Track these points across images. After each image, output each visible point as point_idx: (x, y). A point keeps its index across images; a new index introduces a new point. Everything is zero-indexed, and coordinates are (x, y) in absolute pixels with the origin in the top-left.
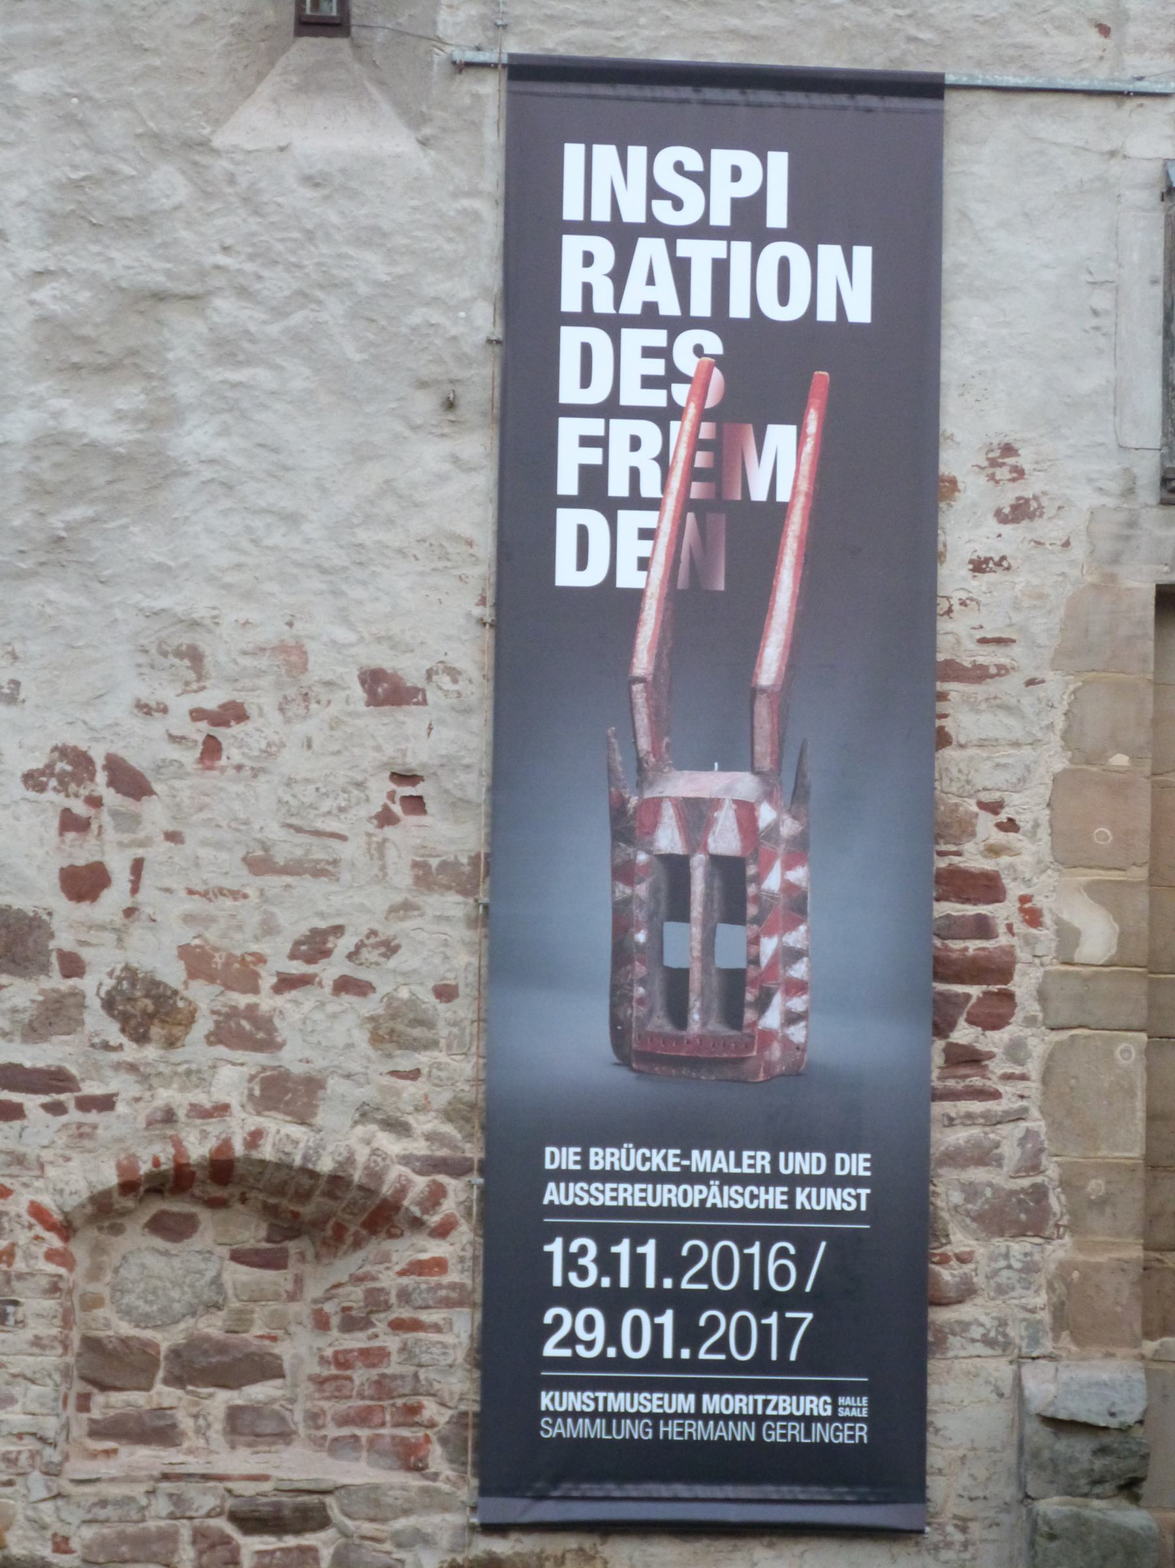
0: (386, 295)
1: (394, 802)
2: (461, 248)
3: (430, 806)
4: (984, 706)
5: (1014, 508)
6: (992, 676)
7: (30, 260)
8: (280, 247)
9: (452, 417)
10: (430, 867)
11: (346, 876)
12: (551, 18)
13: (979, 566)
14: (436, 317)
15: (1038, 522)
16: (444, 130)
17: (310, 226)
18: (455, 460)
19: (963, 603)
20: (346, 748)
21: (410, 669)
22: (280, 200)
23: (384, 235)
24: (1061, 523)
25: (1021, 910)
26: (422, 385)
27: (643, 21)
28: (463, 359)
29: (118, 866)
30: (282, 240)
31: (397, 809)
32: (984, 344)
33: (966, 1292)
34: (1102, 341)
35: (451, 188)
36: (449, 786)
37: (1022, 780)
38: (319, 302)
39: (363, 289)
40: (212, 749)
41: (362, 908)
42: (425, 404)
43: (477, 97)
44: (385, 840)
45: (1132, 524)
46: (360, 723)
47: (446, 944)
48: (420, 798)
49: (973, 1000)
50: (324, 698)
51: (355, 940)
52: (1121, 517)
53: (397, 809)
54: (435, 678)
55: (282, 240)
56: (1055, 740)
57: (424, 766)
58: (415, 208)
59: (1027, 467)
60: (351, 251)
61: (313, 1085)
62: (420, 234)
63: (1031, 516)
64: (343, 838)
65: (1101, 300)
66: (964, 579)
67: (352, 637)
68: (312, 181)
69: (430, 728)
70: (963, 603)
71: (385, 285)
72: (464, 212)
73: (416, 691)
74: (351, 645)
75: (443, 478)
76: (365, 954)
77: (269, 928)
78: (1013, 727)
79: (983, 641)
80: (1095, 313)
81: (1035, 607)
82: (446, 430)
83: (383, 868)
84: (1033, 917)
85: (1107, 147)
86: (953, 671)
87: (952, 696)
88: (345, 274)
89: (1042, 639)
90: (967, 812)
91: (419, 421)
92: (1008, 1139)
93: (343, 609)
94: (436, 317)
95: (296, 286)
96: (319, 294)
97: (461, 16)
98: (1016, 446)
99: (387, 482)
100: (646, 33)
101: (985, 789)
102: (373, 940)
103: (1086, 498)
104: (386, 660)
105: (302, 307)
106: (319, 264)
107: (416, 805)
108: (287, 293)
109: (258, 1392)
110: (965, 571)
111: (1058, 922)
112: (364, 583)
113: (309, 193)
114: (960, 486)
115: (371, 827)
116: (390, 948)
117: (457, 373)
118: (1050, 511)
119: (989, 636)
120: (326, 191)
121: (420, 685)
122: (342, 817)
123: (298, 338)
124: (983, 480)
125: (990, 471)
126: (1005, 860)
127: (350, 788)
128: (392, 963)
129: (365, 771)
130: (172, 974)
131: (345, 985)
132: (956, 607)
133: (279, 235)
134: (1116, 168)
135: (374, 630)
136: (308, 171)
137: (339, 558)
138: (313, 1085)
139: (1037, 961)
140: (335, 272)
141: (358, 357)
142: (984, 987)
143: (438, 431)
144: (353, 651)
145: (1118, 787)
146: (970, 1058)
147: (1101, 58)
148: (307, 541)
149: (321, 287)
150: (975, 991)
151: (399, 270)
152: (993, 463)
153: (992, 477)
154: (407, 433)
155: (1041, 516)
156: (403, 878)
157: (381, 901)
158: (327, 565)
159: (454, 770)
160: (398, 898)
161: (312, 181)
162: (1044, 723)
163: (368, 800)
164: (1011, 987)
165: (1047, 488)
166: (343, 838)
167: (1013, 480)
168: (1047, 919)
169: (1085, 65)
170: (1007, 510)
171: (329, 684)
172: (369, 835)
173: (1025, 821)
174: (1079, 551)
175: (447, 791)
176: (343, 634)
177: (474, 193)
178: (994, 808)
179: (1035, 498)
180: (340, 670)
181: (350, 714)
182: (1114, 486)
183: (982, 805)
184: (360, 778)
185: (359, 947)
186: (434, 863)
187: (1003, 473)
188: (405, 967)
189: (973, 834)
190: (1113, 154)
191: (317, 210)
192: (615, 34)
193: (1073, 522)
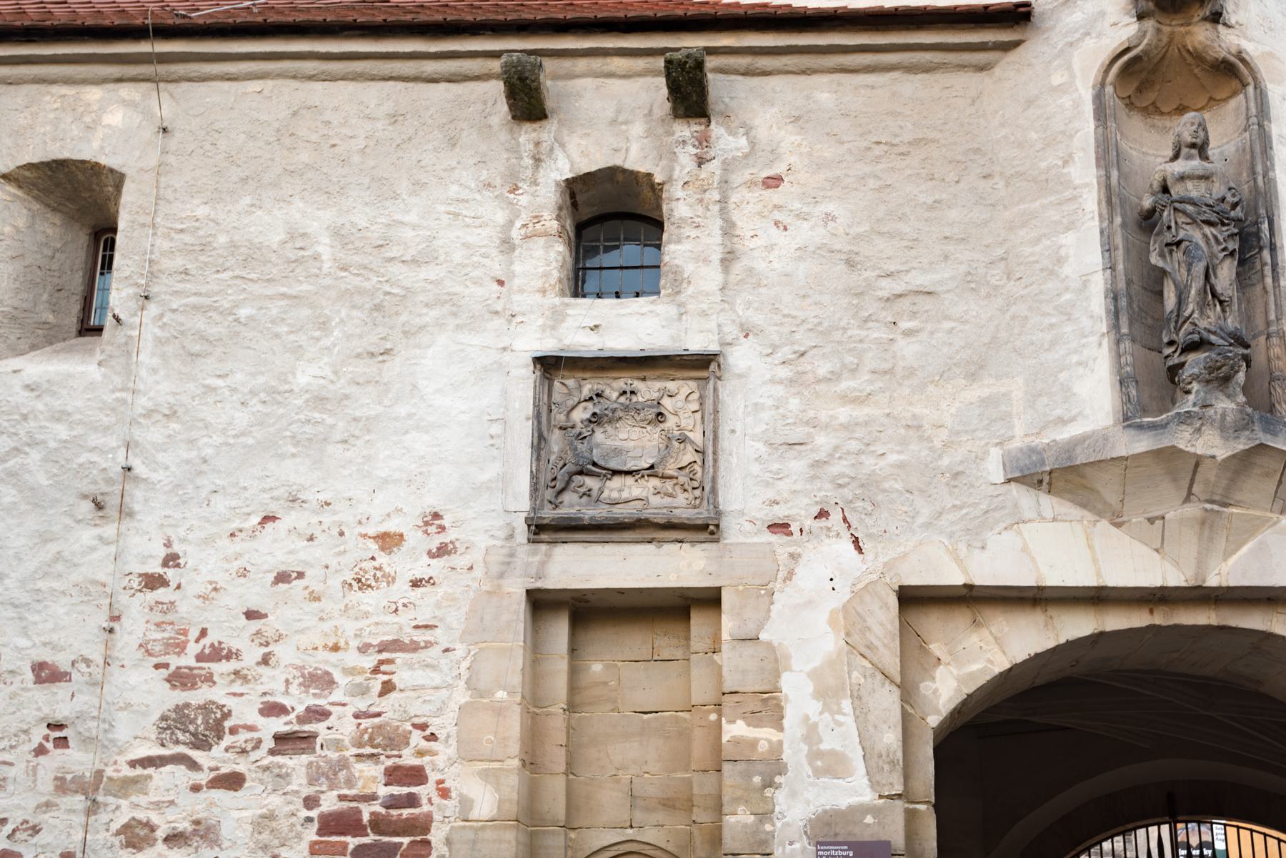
0: (66, 447)
1: (48, 741)
2: (113, 419)
3: (71, 743)
4: (417, 666)
5: (439, 549)
6: (422, 648)
8: (6, 424)
9: (100, 514)
10: (65, 779)
11: (10, 788)
12: (176, 292)
13: (416, 584)
14: (94, 457)
15: (453, 556)
16: (111, 356)
17: (25, 412)
18: (101, 538)
19: (405, 605)
20: (19, 710)
21: (62, 661)
22: (9, 399)
23: (69, 414)
24: (468, 556)
25: (438, 789)
26: (85, 497)
27: (230, 291)
28: (110, 481)
30: (8, 420)
31: (50, 746)
32: (423, 457)
34: (495, 452)
35: (111, 387)
36: (81, 730)
37: (440, 709)
38: (26, 454)
39: (52, 444)
41: (18, 807)
43: (131, 337)
44: (38, 764)
45: (512, 555)
46: (29, 694)
47: (71, 826)
48: (66, 738)
49: (404, 847)
50: (9, 681)
51: (14, 826)
52: (504, 551)
53: (50, 746)
54: (76, 665)
55: (8, 420)
56: (462, 684)
57: (67, 718)
58: (89, 399)
59: (447, 525)
60: (48, 424)
62: (90, 413)
63: (449, 553)
64: (11, 764)
65: (496, 429)
66: (406, 591)
67: (28, 643)
68: (29, 388)
69: (73, 696)
70: (405, 605)
71: (65, 441)
72: (117, 400)
73: (66, 674)
74: (27, 648)
75: (93, 549)
76: (18, 835)
78: (436, 678)
79: (417, 627)
80: (492, 437)
81: (450, 606)
82: (98, 522)
83: (35, 781)
84: (445, 793)
85: (502, 345)
87: (398, 661)
88: (43, 437)
89: (455, 625)
90: (404, 731)
91: (80, 517)
93: (25, 628)
94: (94, 457)
95: (13, 445)
96: (27, 449)
97: (124, 294)
98: (441, 513)
99: (58, 553)
100: (232, 298)
101: (416, 716)
102: (25, 826)
103: (482, 542)
104: (47, 656)
105: (15, 457)
106: (28, 432)
107: (62, 742)
108: (7, 449)
110: (407, 586)
111: (461, 795)
112: (39, 612)
113: (26, 394)
114: (405, 537)
115: (30, 757)
116: (35, 830)
117: (105, 489)
118: (461, 549)
119: (420, 624)
120: (36, 393)
121: (68, 670)
122: (12, 751)
123: (12, 474)
124: (420, 533)
125: (425, 528)
126: (427, 759)
127: (20, 734)
128: (35, 840)
129: (29, 723)
132: (401, 608)
133: (6, 418)
134: (507, 357)
135: (43, 639)
136: (27, 383)
137: (25, 598)
139: (446, 820)
140: (36, 436)
141: (46, 483)
142: (412, 838)
143: (93, 523)
144: (28, 652)
145: (499, 711)
147: (499, 298)
148: (7, 589)
149: (29, 445)
150: (406, 840)
151: (75, 433)
152: (427, 524)
153: (426, 532)
154: (73, 524)
155: (455, 553)
156: (46, 785)
157: (32, 804)
158: (17, 602)
159: (85, 720)
160: (44, 799)
161: (29, 388)
162: (454, 675)
163: (30, 740)
164: (429, 837)
165: (459, 537)
166: (11, 764)
167: (439, 533)
168: (453, 794)
169: (489, 302)
170: (434, 551)
171: (12, 672)
172: (28, 762)
173: (441, 735)
174: (479, 572)
175: (80, 733)
176: (23, 642)
177: (122, 390)
178: (423, 727)
179: (451, 542)
180: (19, 663)
181: (23, 689)
182: (502, 534)
183: (414, 726)
184: (25, 727)
185: (14, 831)
186: (69, 777)
187: (432, 529)
188: (43, 842)
189: (408, 744)
190: (505, 349)
191: (31, 403)
192: (215, 299)
193: (476, 556)
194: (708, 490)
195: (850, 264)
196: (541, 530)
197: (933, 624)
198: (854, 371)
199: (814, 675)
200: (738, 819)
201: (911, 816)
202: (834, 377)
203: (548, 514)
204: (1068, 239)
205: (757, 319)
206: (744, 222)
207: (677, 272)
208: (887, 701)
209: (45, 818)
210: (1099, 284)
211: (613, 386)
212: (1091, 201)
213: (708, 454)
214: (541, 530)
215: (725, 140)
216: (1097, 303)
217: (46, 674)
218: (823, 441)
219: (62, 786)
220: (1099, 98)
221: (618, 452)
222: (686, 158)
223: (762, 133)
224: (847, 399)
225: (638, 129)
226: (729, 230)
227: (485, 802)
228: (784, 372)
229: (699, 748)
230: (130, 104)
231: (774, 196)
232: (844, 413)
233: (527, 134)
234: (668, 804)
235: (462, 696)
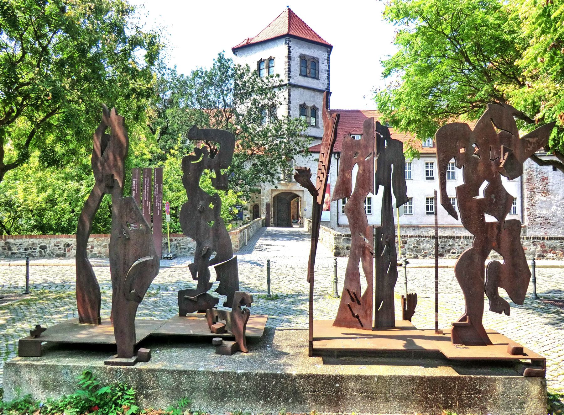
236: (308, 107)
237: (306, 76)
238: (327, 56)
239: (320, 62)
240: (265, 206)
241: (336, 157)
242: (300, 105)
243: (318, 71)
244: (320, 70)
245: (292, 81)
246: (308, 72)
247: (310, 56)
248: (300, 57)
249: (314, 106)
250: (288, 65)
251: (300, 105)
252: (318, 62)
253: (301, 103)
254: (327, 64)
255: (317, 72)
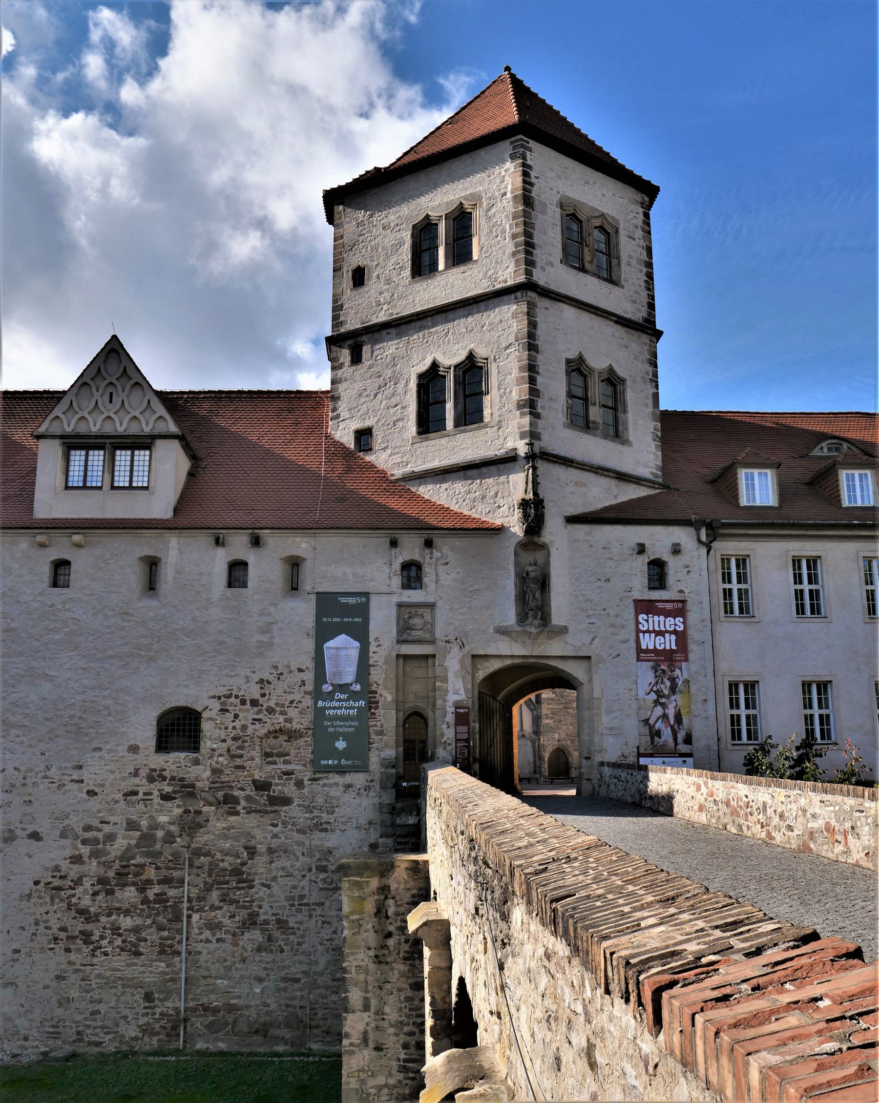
7: (257, 619)
29: (267, 693)
33: (373, 743)
40: (279, 678)
42: (305, 635)
61: (292, 720)
77: (286, 700)
86: (371, 666)
92: (379, 724)
109: (287, 758)
130: (274, 706)
131: (295, 707)
138: (292, 720)
146: (374, 714)
156: (302, 694)
157: (300, 696)
194: (432, 632)
195: (463, 583)
196: (400, 642)
197: (477, 661)
198: (463, 607)
199: (454, 673)
200: (439, 702)
201: (473, 701)
202: (459, 609)
203: (401, 639)
204: (508, 581)
205: (443, 595)
206: (440, 574)
207: (426, 584)
208: (469, 678)
209: (302, 700)
210: (513, 593)
211: (413, 611)
212: (513, 574)
213: (433, 625)
214: (400, 642)
215: (436, 554)
216: (513, 597)
217: (300, 670)
218: (457, 623)
219: (306, 693)
220: (515, 551)
221: (414, 625)
222: (428, 557)
223: (444, 551)
224: (462, 614)
225: (417, 550)
226: (437, 574)
227: (389, 698)
228: (448, 607)
229: (430, 688)
230: (306, 542)
231: (446, 567)
232: (461, 617)
233: (394, 551)
234: (423, 698)
235: (383, 676)
236: (591, 370)
237: (582, 269)
238: (641, 217)
239: (622, 233)
240: (450, 718)
241: (704, 538)
242: (568, 361)
243: (618, 258)
244: (624, 258)
245: (540, 277)
246: (587, 258)
247: (593, 209)
248: (561, 206)
249: (611, 370)
250: (525, 224)
251: (568, 361)
252: (617, 232)
253: (573, 355)
254: (643, 243)
255: (614, 262)
